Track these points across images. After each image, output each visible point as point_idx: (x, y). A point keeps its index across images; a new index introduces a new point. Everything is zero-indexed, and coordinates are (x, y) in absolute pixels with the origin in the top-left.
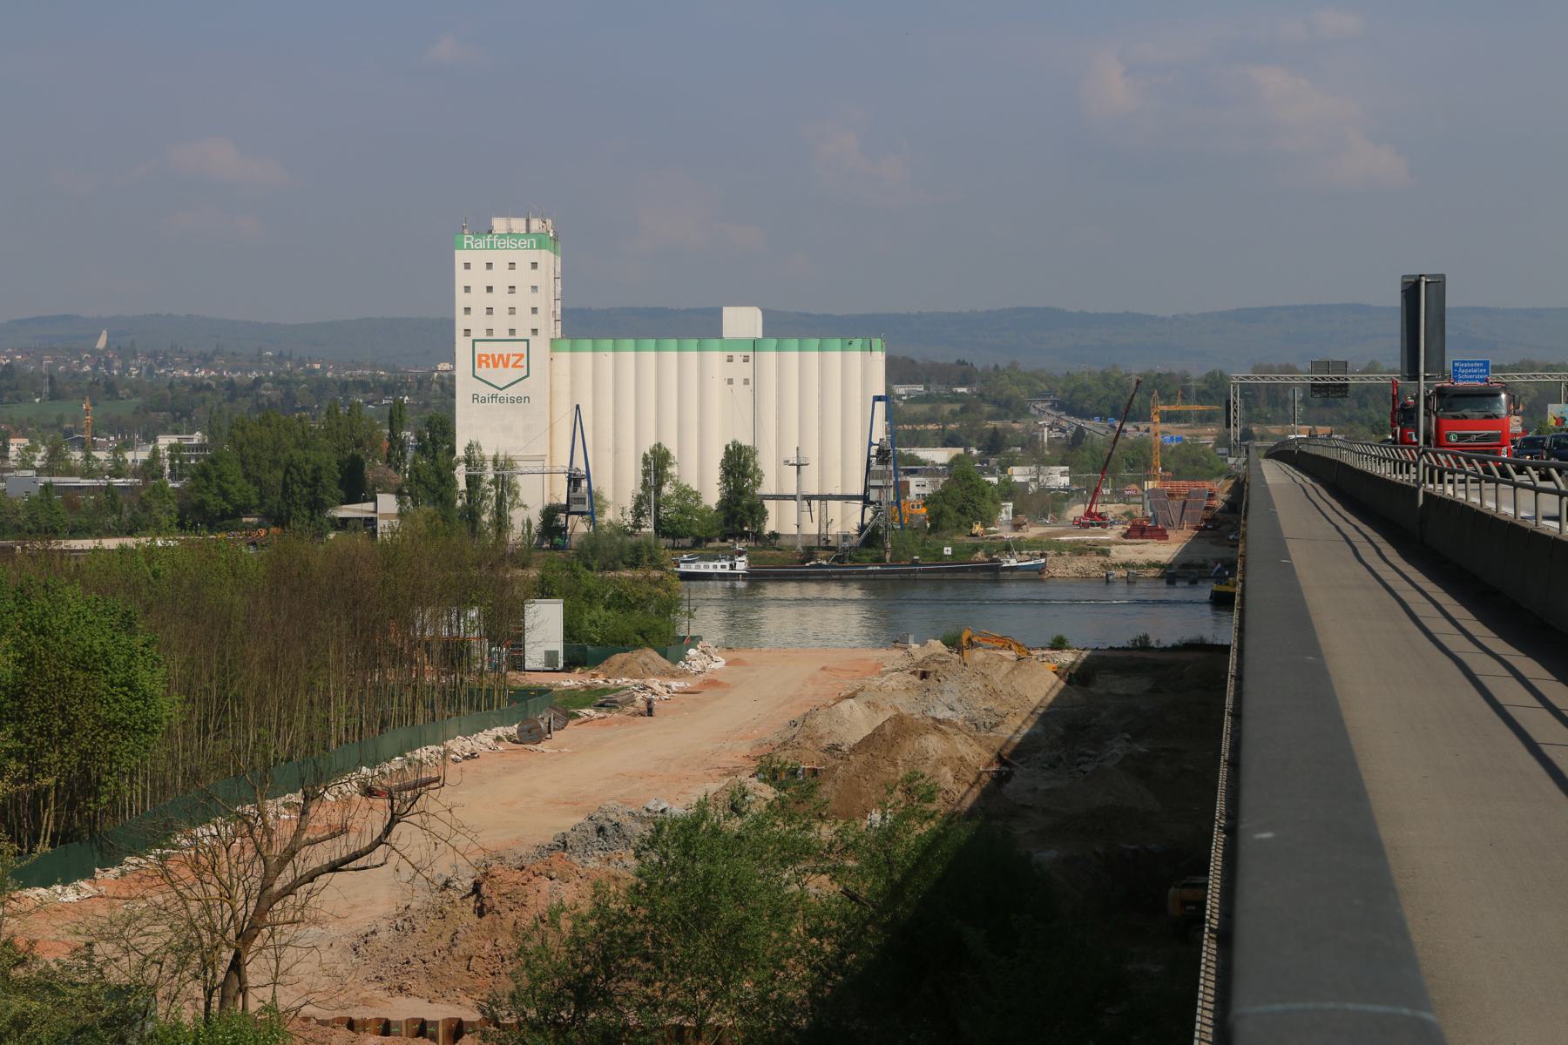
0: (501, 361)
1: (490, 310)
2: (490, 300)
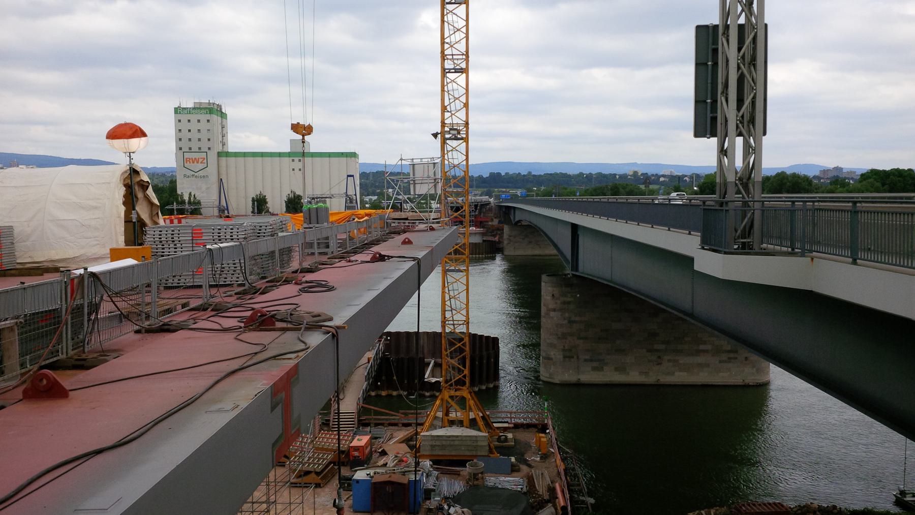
1: (190, 140)
2: (189, 135)
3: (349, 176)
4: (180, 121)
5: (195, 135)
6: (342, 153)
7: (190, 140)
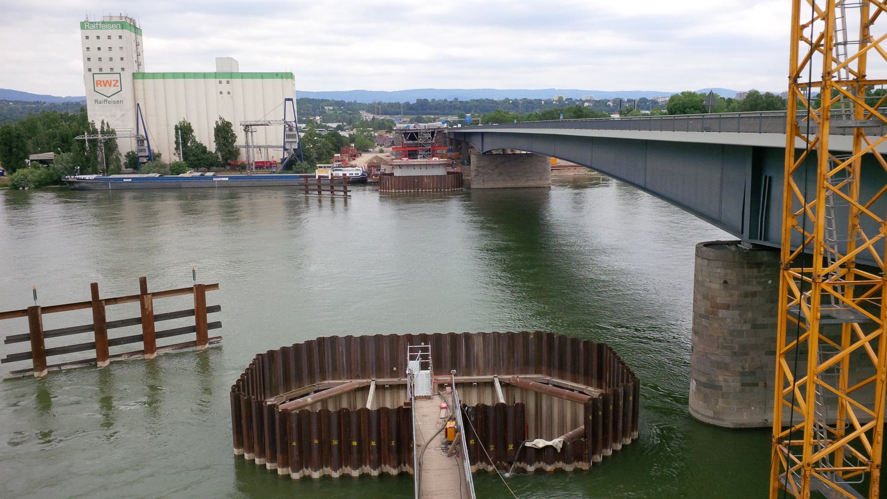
0: (107, 83)
3: (287, 100)
4: (87, 37)
6: (277, 74)
7: (100, 59)
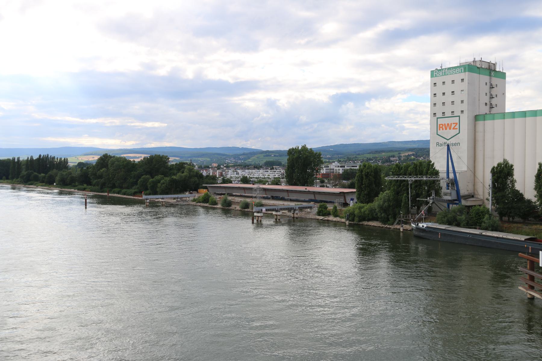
0: (448, 127)
5: (449, 98)
